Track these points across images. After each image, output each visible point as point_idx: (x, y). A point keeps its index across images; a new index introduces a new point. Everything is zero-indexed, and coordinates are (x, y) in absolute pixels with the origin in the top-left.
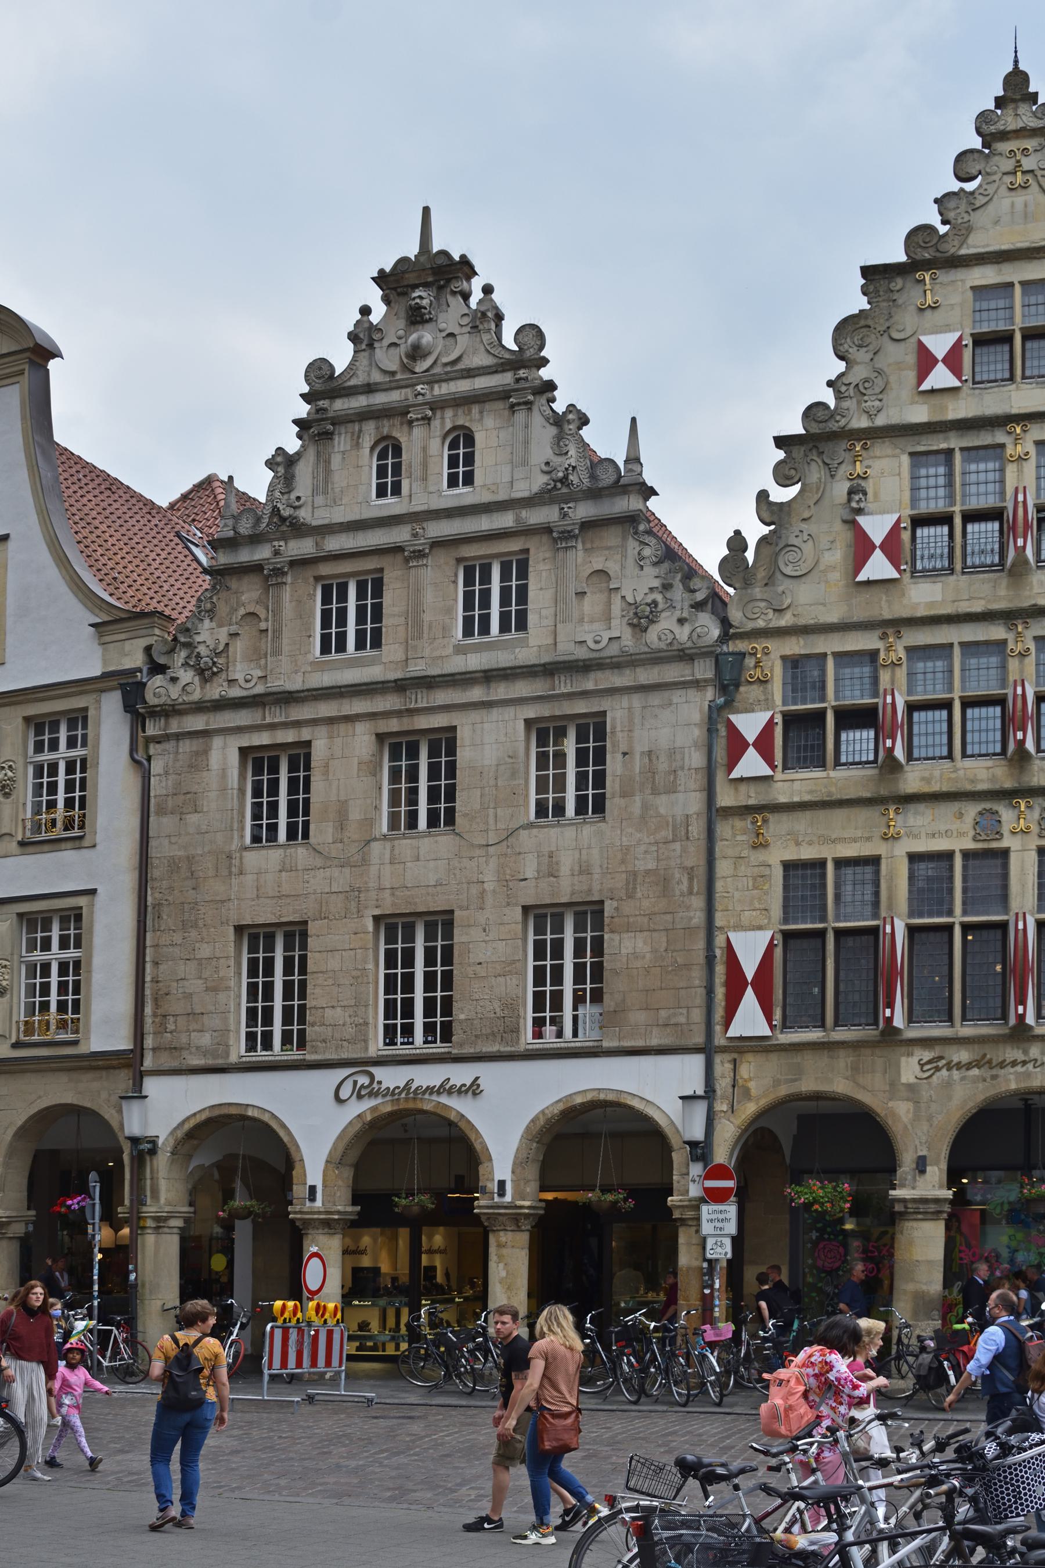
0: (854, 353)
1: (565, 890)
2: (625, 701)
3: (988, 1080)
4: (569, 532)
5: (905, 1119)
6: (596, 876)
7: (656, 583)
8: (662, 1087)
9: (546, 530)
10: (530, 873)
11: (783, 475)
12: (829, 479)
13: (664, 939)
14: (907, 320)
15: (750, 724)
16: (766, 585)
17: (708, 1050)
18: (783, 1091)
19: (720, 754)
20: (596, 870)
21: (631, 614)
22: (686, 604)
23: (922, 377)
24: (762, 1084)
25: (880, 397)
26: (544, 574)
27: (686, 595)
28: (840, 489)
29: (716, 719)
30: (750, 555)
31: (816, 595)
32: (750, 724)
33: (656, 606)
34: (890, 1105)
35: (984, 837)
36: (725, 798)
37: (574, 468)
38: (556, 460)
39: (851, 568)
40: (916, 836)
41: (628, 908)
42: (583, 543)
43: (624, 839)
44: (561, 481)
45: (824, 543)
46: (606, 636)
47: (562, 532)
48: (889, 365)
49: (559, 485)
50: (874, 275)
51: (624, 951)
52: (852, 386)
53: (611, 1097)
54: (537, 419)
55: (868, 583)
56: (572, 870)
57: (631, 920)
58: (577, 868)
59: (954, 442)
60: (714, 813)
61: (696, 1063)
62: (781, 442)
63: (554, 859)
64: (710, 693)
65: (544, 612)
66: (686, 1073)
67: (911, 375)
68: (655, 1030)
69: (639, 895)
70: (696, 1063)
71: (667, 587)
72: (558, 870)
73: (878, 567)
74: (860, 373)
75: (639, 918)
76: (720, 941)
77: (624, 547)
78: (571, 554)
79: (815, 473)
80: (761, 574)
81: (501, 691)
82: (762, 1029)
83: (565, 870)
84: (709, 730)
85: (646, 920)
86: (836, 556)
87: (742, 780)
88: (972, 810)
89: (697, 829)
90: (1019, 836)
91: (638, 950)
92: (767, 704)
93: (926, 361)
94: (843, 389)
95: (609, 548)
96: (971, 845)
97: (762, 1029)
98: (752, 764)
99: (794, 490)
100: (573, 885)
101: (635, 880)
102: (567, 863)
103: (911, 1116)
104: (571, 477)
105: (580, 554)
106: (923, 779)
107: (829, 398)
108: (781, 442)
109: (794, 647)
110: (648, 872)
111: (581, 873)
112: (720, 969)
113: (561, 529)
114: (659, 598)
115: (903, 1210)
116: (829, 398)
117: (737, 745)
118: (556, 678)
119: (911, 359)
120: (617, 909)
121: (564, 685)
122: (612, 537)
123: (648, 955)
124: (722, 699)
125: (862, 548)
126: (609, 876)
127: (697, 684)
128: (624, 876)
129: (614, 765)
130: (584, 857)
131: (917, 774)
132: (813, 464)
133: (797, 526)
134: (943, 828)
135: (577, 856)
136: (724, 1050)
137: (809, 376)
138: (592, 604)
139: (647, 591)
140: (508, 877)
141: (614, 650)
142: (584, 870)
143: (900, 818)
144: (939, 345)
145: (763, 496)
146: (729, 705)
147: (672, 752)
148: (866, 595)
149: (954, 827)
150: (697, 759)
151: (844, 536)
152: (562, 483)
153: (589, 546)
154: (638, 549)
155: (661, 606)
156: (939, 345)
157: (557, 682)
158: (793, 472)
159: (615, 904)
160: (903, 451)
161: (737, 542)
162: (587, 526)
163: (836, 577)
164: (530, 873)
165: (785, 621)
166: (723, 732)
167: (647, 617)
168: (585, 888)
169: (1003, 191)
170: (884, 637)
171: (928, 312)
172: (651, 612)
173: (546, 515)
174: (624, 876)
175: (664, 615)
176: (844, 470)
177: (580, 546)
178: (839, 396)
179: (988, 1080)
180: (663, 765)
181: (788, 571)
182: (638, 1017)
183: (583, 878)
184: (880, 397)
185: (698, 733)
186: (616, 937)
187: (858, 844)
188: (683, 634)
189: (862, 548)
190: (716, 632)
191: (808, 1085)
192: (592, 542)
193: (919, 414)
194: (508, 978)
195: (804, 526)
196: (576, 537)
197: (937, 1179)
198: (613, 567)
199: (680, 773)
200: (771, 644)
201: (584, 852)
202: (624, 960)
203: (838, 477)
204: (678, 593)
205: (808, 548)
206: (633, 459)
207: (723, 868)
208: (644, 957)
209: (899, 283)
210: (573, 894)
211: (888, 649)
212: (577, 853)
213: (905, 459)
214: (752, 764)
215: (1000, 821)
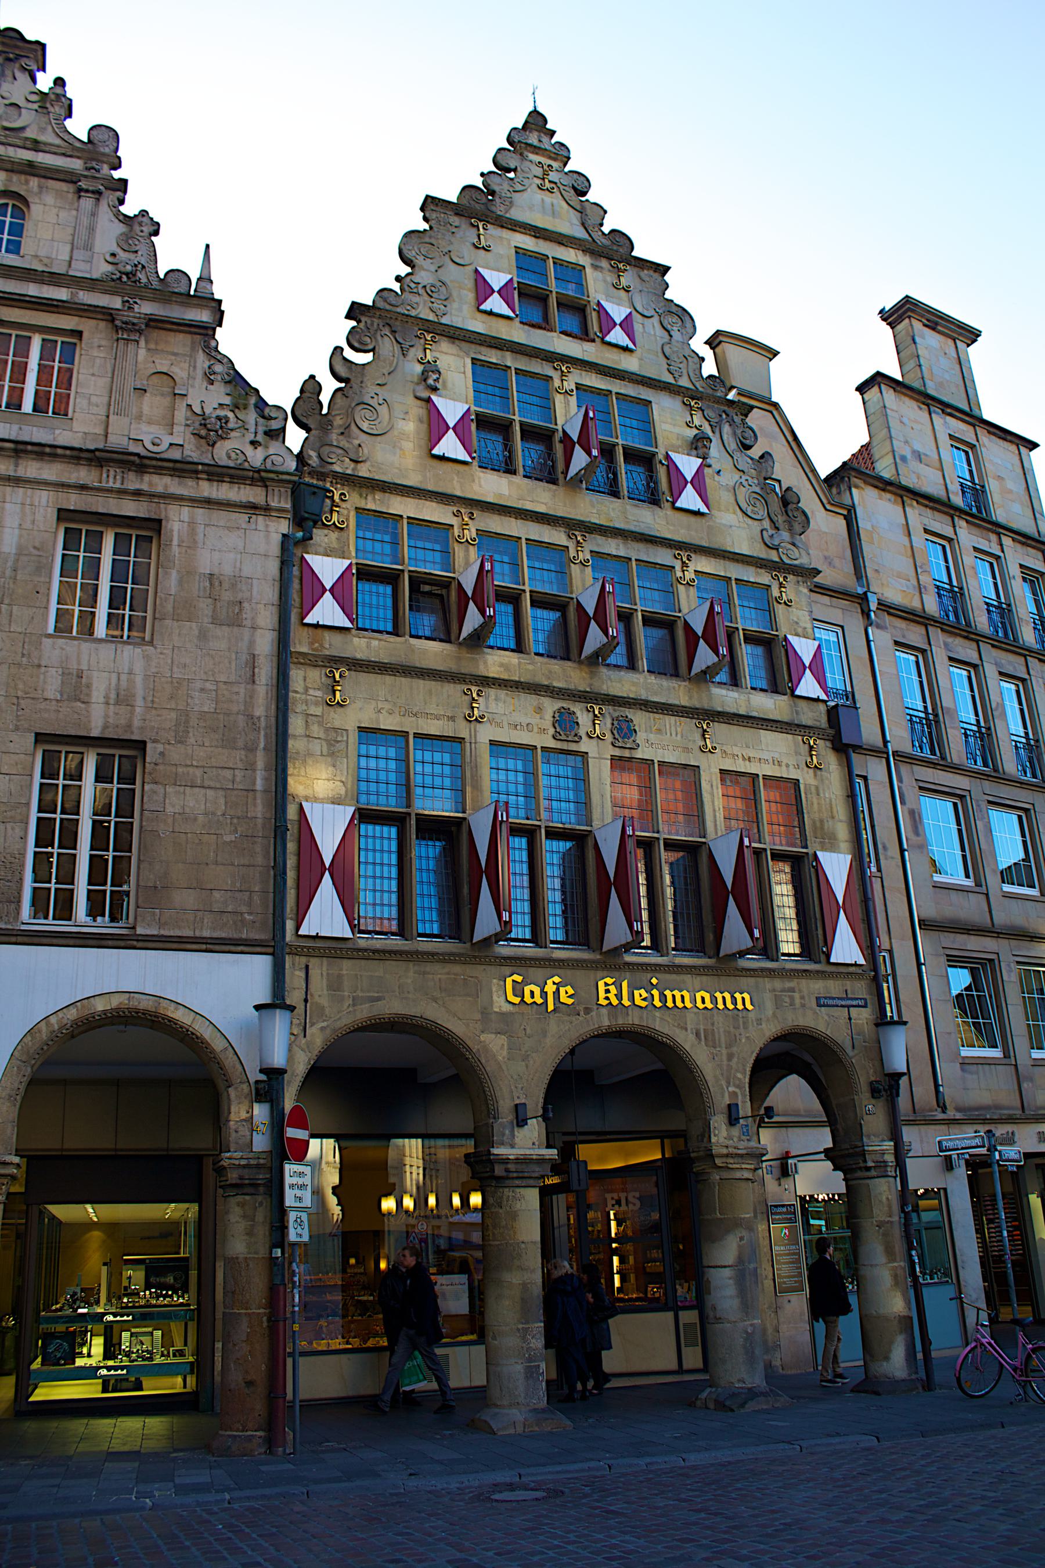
0: (419, 261)
1: (97, 720)
3: (582, 1013)
4: (134, 324)
5: (502, 1055)
6: (138, 710)
7: (227, 400)
8: (219, 993)
9: (108, 315)
11: (354, 340)
12: (402, 357)
13: (222, 801)
15: (328, 569)
16: (342, 433)
17: (275, 947)
18: (364, 1013)
20: (139, 702)
21: (197, 424)
22: (261, 429)
24: (339, 1003)
25: (445, 303)
26: (98, 361)
27: (261, 420)
32: (328, 569)
33: (226, 423)
34: (482, 1039)
35: (563, 737)
37: (143, 267)
38: (122, 255)
39: (424, 442)
40: (499, 725)
41: (176, 754)
42: (147, 342)
43: (175, 669)
44: (127, 274)
46: (167, 440)
47: (126, 323)
48: (452, 281)
49: (125, 278)
51: (169, 810)
52: (420, 286)
53: (145, 1004)
54: (105, 212)
55: (442, 458)
56: (107, 697)
57: (180, 770)
58: (113, 696)
60: (284, 656)
61: (260, 966)
63: (84, 680)
65: (94, 399)
66: (247, 977)
67: (470, 296)
68: (208, 919)
69: (192, 740)
70: (260, 966)
71: (235, 407)
72: (89, 695)
73: (450, 446)
74: (424, 277)
75: (191, 770)
76: (292, 813)
77: (192, 356)
78: (131, 347)
79: (387, 346)
80: (338, 421)
81: (31, 469)
82: (340, 928)
83: (97, 695)
84: (282, 563)
85: (198, 773)
86: (409, 426)
87: (316, 626)
88: (551, 706)
90: (594, 742)
91: (187, 810)
93: (483, 289)
94: (413, 285)
95: (175, 354)
96: (552, 744)
97: (340, 928)
99: (368, 357)
100: (106, 716)
101: (187, 722)
102: (100, 688)
103: (505, 1053)
104: (139, 274)
105: (142, 352)
106: (501, 665)
110: (203, 715)
111: (117, 703)
112: (291, 846)
113: (125, 319)
114: (231, 415)
115: (504, 1174)
118: (105, 470)
119: (470, 283)
120: (162, 754)
121: (112, 479)
122: (180, 342)
123: (201, 818)
124: (301, 534)
125: (436, 426)
126: (154, 712)
127: (266, 510)
128: (173, 715)
130: (124, 684)
131: (496, 658)
132: (386, 339)
134: (524, 720)
135: (114, 681)
136: (296, 952)
138: (152, 404)
139: (216, 406)
140: (20, 694)
141: (176, 454)
142: (123, 699)
143: (481, 700)
144: (497, 279)
145: (338, 349)
149: (533, 721)
151: (417, 410)
152: (128, 278)
153: (152, 346)
154: (208, 364)
155: (231, 425)
156: (497, 279)
157: (105, 475)
158: (368, 340)
159: (160, 747)
160: (468, 355)
161: (311, 387)
162: (154, 323)
166: (296, 571)
167: (216, 431)
168: (123, 722)
169: (534, 187)
170: (457, 514)
171: (482, 252)
172: (221, 427)
174: (173, 715)
175: (233, 434)
176: (416, 353)
177: (142, 343)
179: (582, 1013)
181: (365, 426)
182: (185, 899)
183: (123, 709)
184: (445, 303)
186: (160, 789)
187: (441, 722)
191: (393, 1006)
192: (157, 344)
194: (9, 826)
195: (378, 390)
196: (140, 332)
197: (536, 1134)
198: (180, 372)
199: (246, 605)
201: (124, 677)
202: (170, 820)
203: (408, 358)
204: (251, 417)
205: (383, 410)
206: (206, 279)
207: (296, 724)
208: (195, 819)
209: (455, 220)
210: (105, 727)
211: (464, 526)
212: (114, 676)
213: (469, 361)
214: (327, 611)
215: (577, 723)
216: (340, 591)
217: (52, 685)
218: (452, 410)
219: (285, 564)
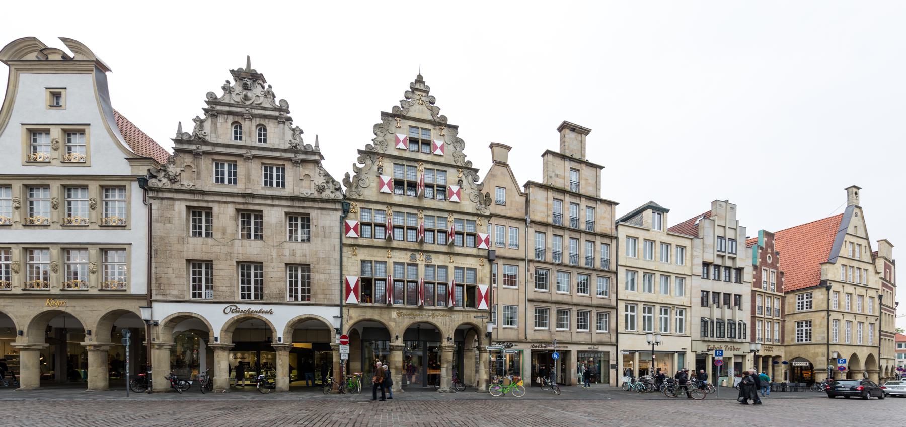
0: (378, 133)
1: (298, 260)
2: (316, 211)
10: (287, 254)
11: (361, 161)
14: (392, 129)
15: (352, 223)
19: (344, 230)
23: (397, 144)
28: (376, 168)
29: (342, 219)
30: (351, 180)
31: (370, 193)
32: (352, 223)
36: (345, 241)
45: (372, 180)
50: (384, 114)
55: (383, 193)
59: (405, 163)
62: (360, 151)
64: (340, 213)
67: (394, 144)
73: (385, 189)
74: (380, 139)
79: (369, 162)
86: (374, 185)
89: (338, 248)
92: (356, 218)
98: (352, 233)
102: (299, 253)
107: (372, 143)
108: (360, 151)
109: (363, 205)
116: (372, 143)
117: (348, 228)
125: (381, 184)
127: (336, 210)
129: (312, 228)
133: (364, 175)
137: (366, 138)
144: (402, 137)
146: (345, 217)
147: (330, 227)
148: (383, 196)
150: (337, 230)
151: (377, 180)
156: (402, 137)
163: (375, 190)
164: (287, 254)
165: (361, 198)
173: (292, 155)
176: (377, 163)
178: (375, 144)
180: (327, 231)
185: (338, 224)
188: (332, 196)
189: (381, 184)
190: (342, 197)
193: (396, 153)
200: (358, 204)
209: (390, 119)
214: (352, 233)
216: (355, 228)
217: (287, 253)
218: (386, 179)
219: (341, 222)
